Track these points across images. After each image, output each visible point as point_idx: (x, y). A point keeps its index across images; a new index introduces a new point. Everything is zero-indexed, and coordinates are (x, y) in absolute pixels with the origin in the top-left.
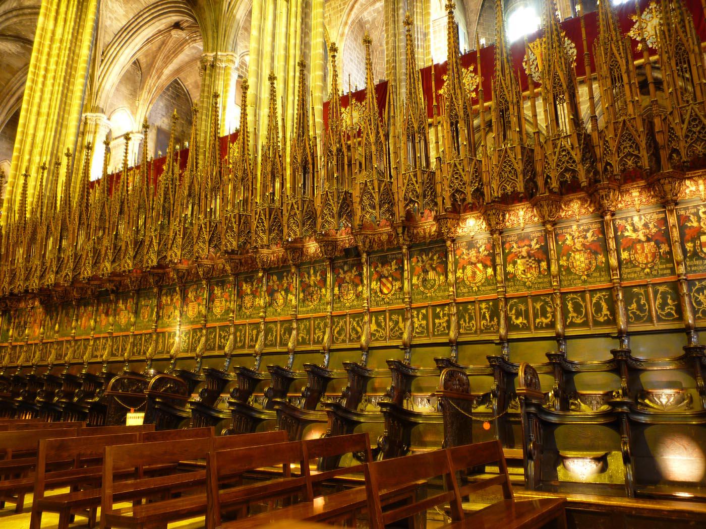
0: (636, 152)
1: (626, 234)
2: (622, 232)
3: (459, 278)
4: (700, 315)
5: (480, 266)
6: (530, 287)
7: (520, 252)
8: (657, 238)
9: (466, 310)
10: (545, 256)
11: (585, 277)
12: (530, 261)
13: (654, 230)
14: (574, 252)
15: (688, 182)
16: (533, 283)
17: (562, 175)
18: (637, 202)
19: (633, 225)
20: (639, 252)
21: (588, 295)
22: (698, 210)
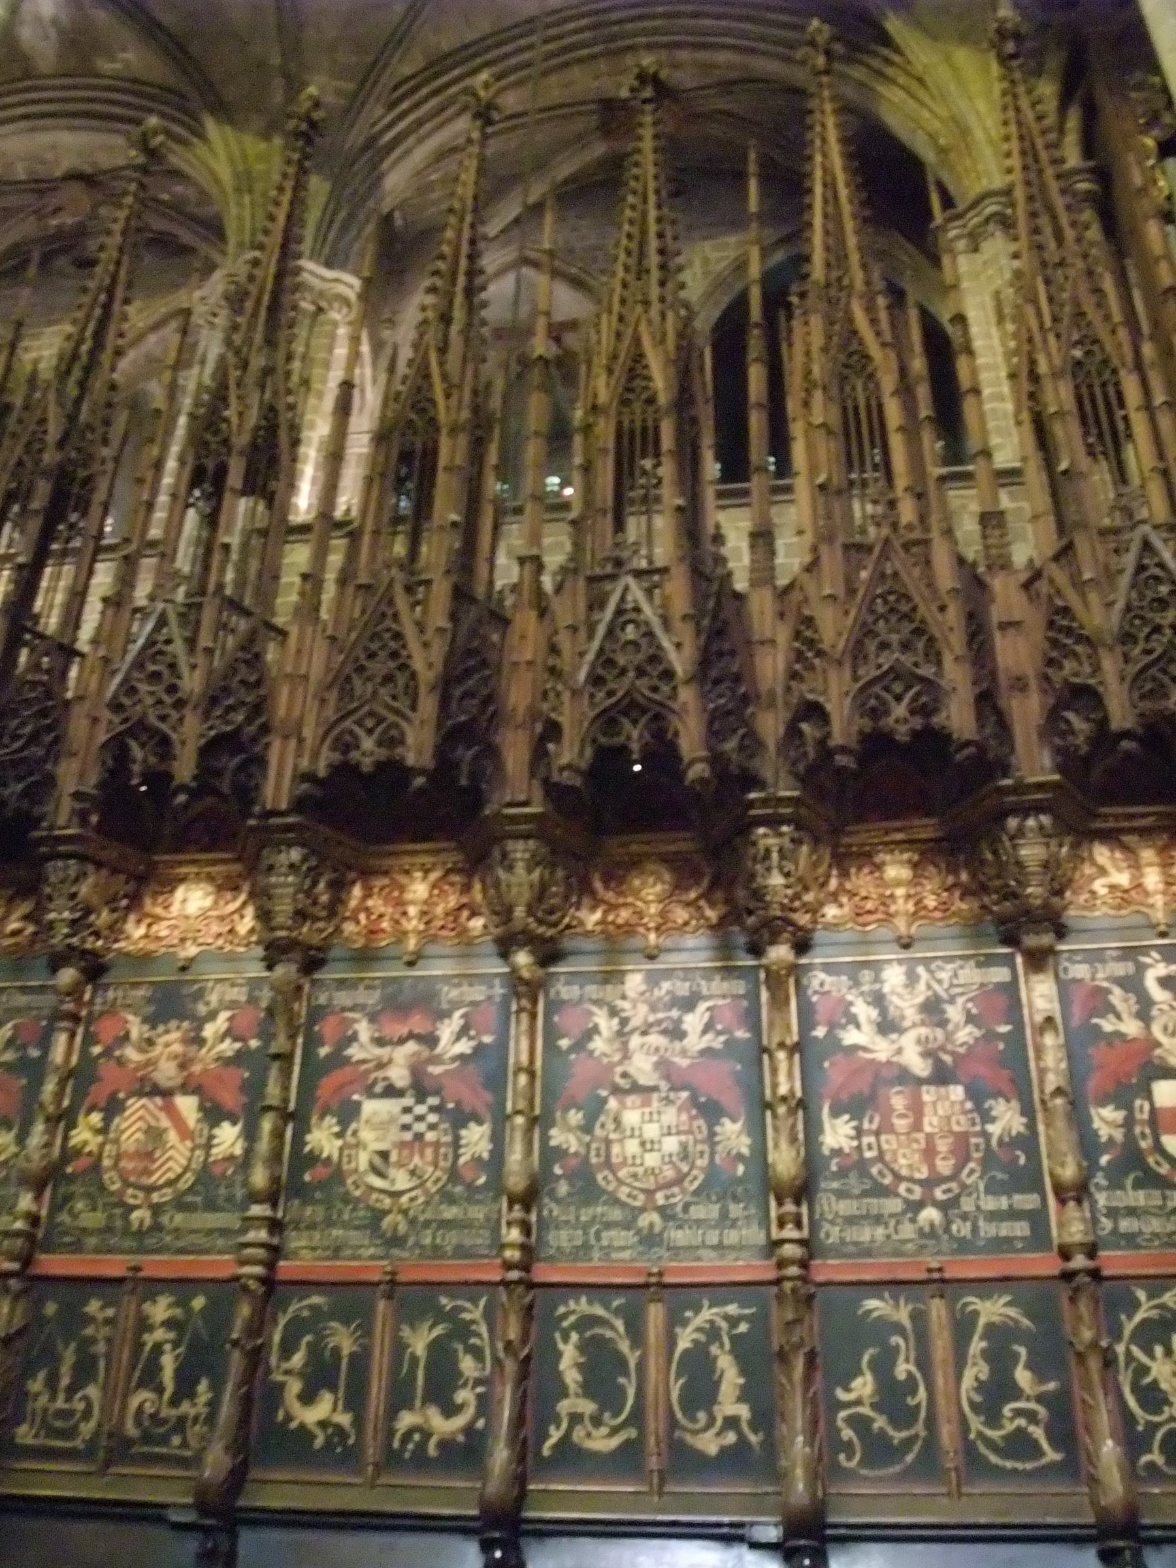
0: (927, 671)
1: (851, 1037)
2: (833, 1026)
3: (78, 1152)
4: (1155, 1457)
5: (187, 1105)
6: (396, 1241)
7: (381, 1065)
8: (981, 1070)
9: (73, 1319)
10: (488, 1097)
11: (655, 1217)
12: (420, 1109)
13: (966, 1034)
14: (616, 1090)
15: (1102, 853)
16: (412, 1222)
17: (608, 720)
18: (902, 905)
19: (878, 1000)
20: (901, 1124)
21: (655, 1314)
22: (1141, 969)
